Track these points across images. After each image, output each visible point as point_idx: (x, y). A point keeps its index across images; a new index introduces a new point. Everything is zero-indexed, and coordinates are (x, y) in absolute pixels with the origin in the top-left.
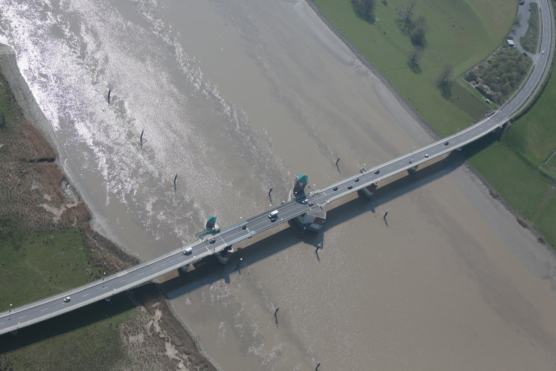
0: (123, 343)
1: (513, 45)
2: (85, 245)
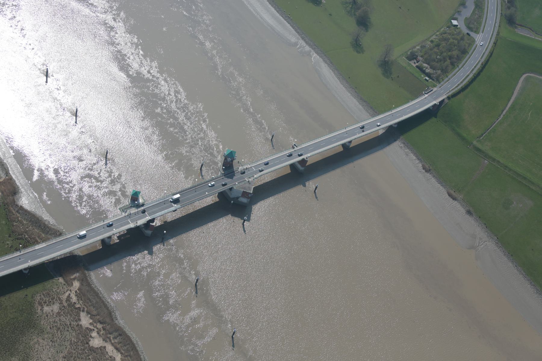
0: (37, 313)
1: (457, 26)
2: (7, 219)
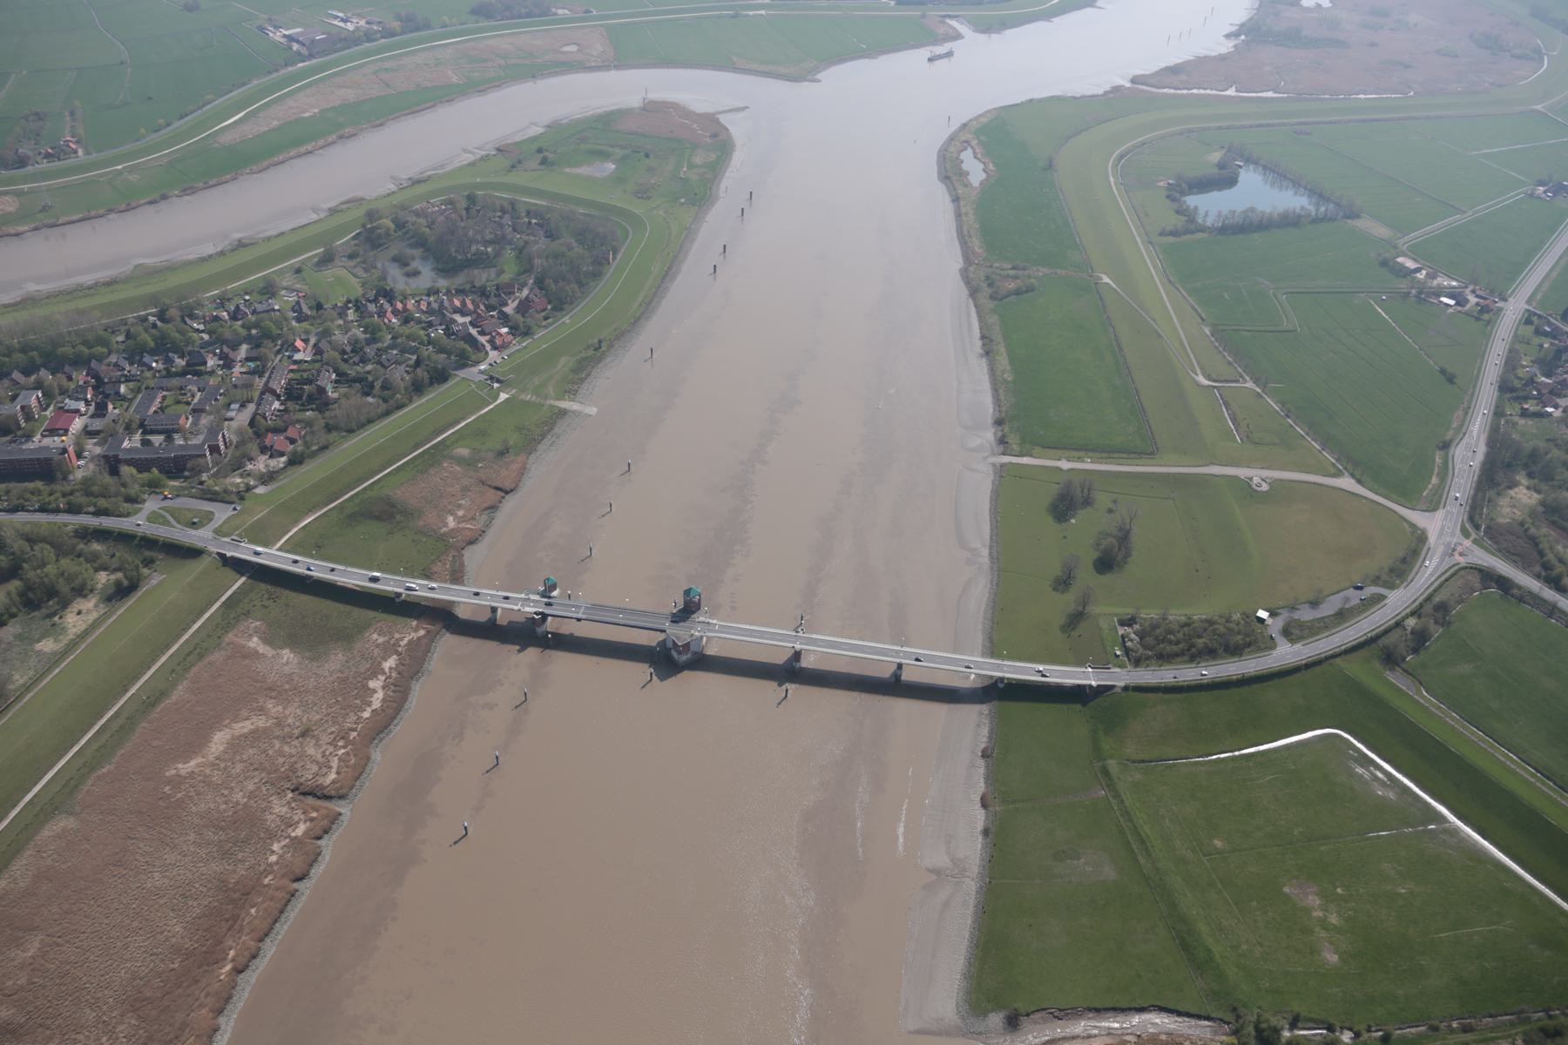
1: (1265, 620)
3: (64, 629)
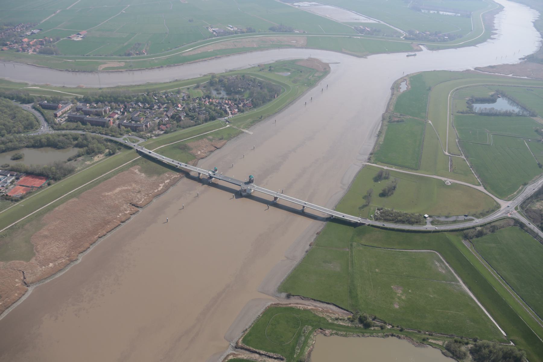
3: (93, 160)
